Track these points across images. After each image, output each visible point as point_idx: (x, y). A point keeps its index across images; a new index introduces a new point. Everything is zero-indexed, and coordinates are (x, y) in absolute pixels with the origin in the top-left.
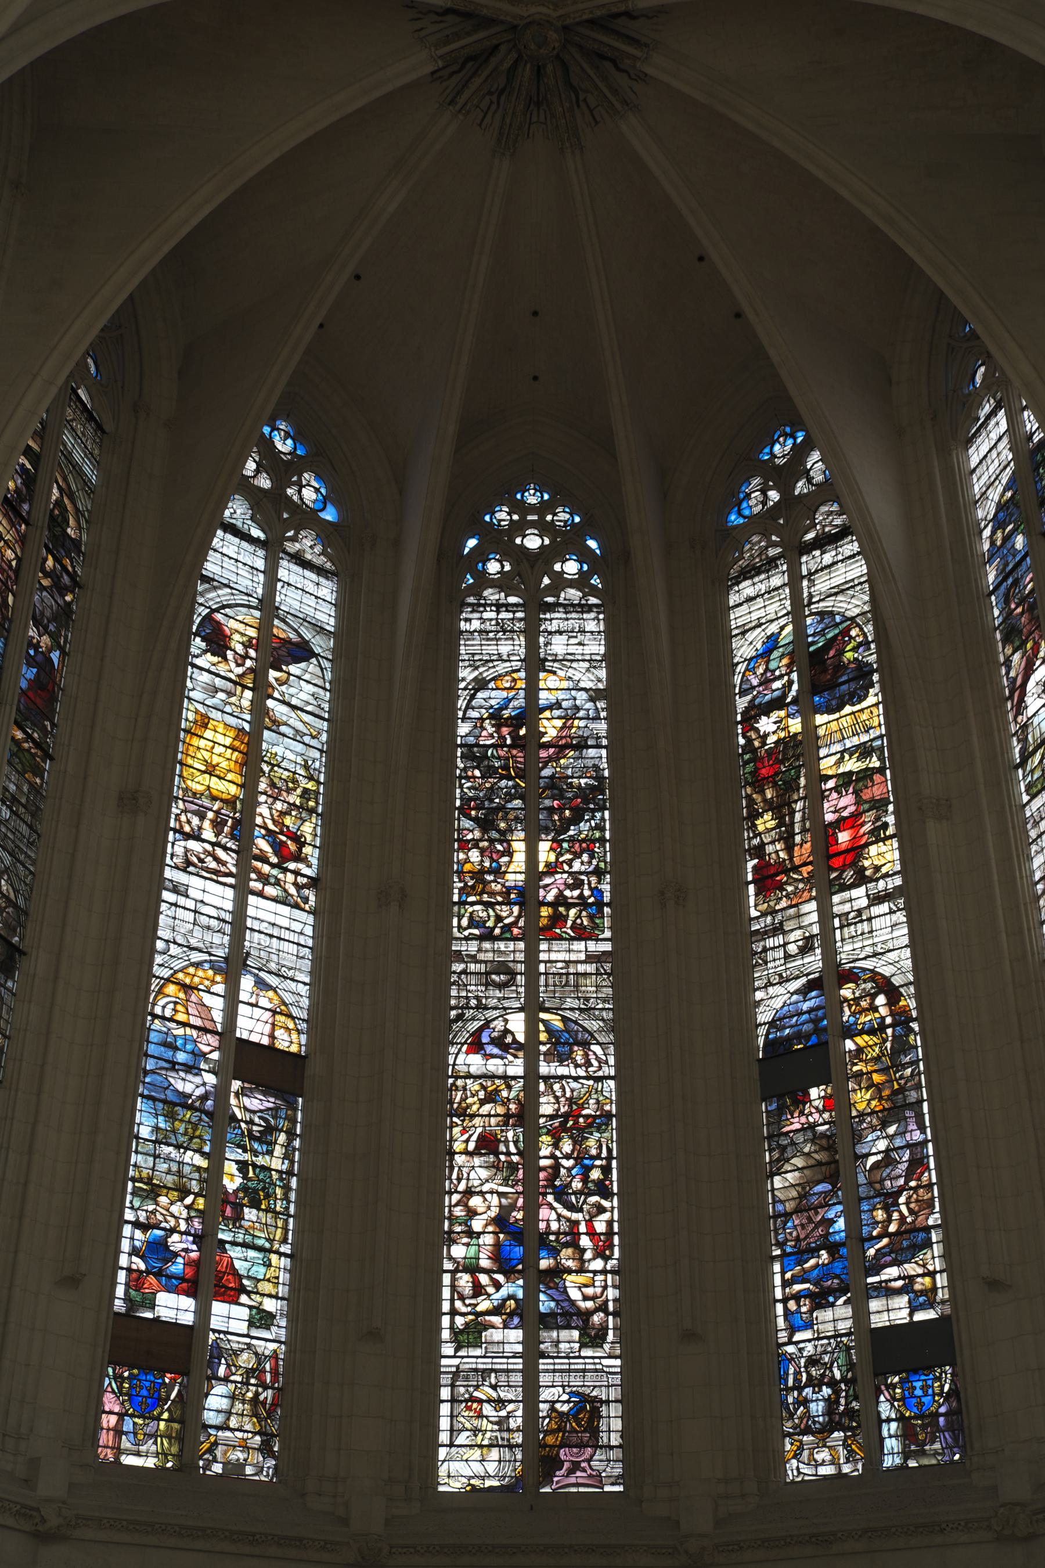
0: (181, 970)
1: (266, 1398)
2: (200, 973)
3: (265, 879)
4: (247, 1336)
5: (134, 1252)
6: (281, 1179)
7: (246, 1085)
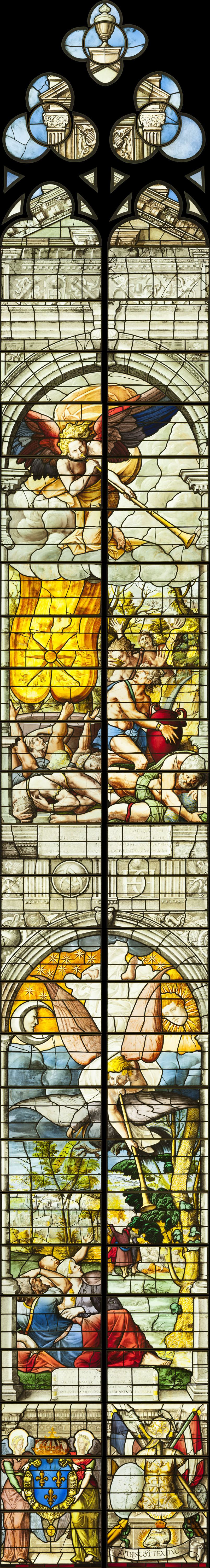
0: (39, 962)
1: (188, 1470)
2: (64, 958)
3: (130, 797)
4: (159, 1402)
5: (20, 1328)
6: (187, 1201)
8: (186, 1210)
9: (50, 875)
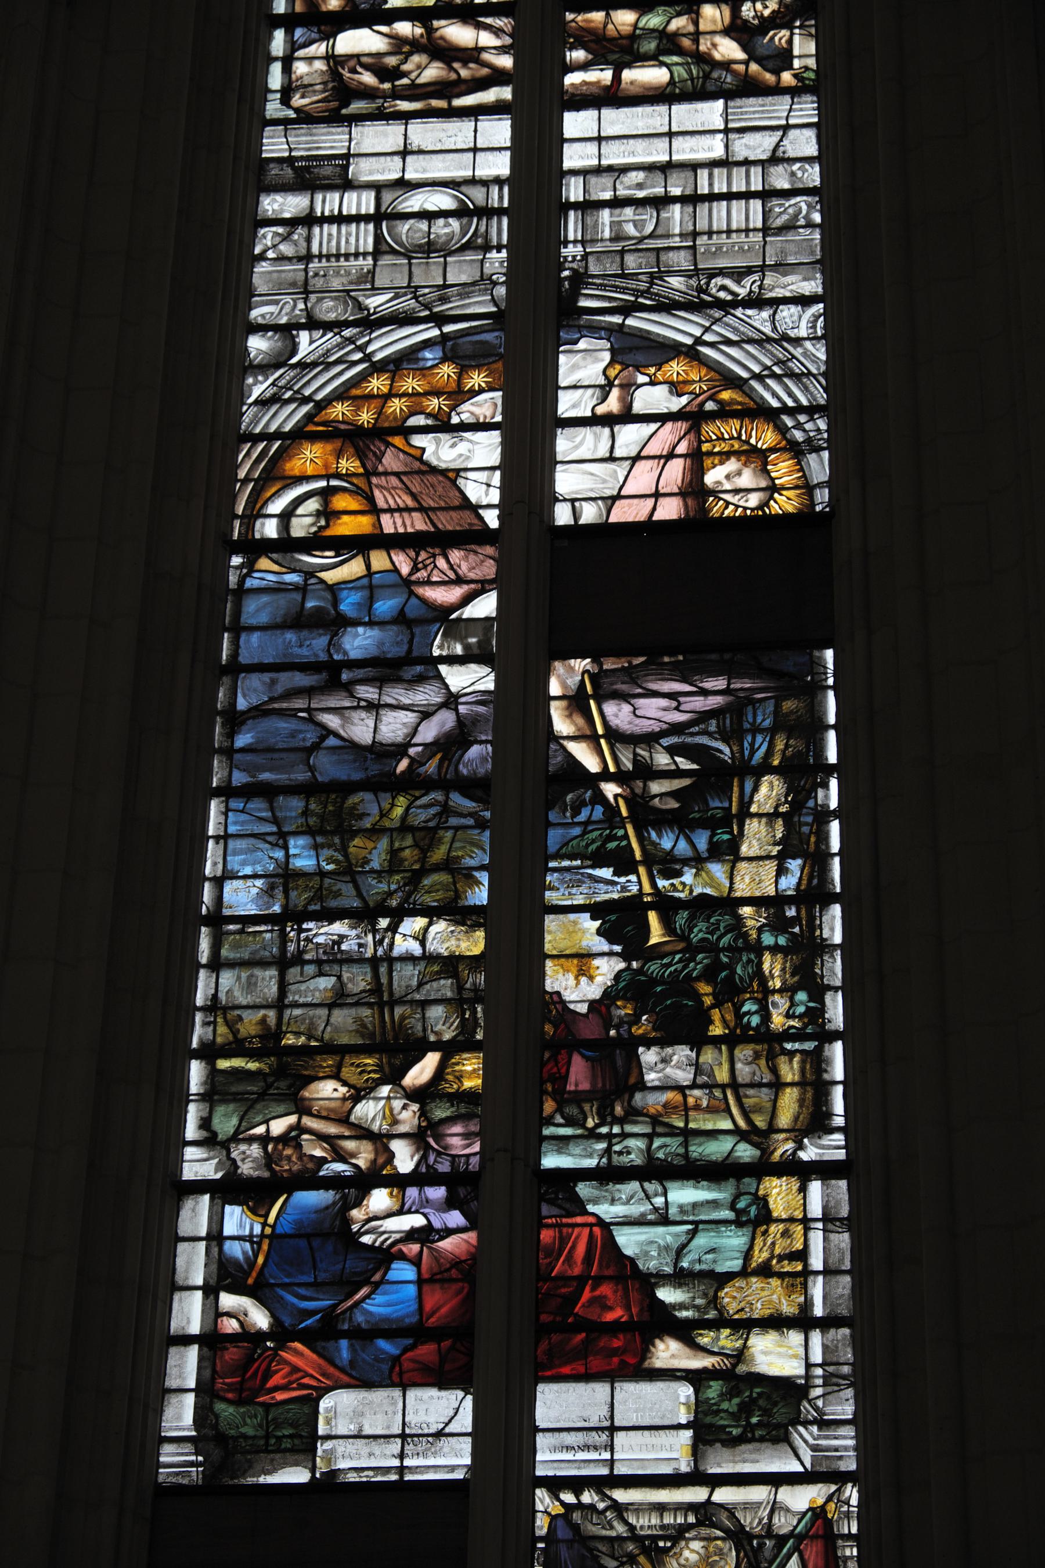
0: (340, 395)
2: (410, 384)
4: (696, 1478)
5: (226, 1275)
7: (609, 664)
8: (775, 949)
9: (377, 218)
